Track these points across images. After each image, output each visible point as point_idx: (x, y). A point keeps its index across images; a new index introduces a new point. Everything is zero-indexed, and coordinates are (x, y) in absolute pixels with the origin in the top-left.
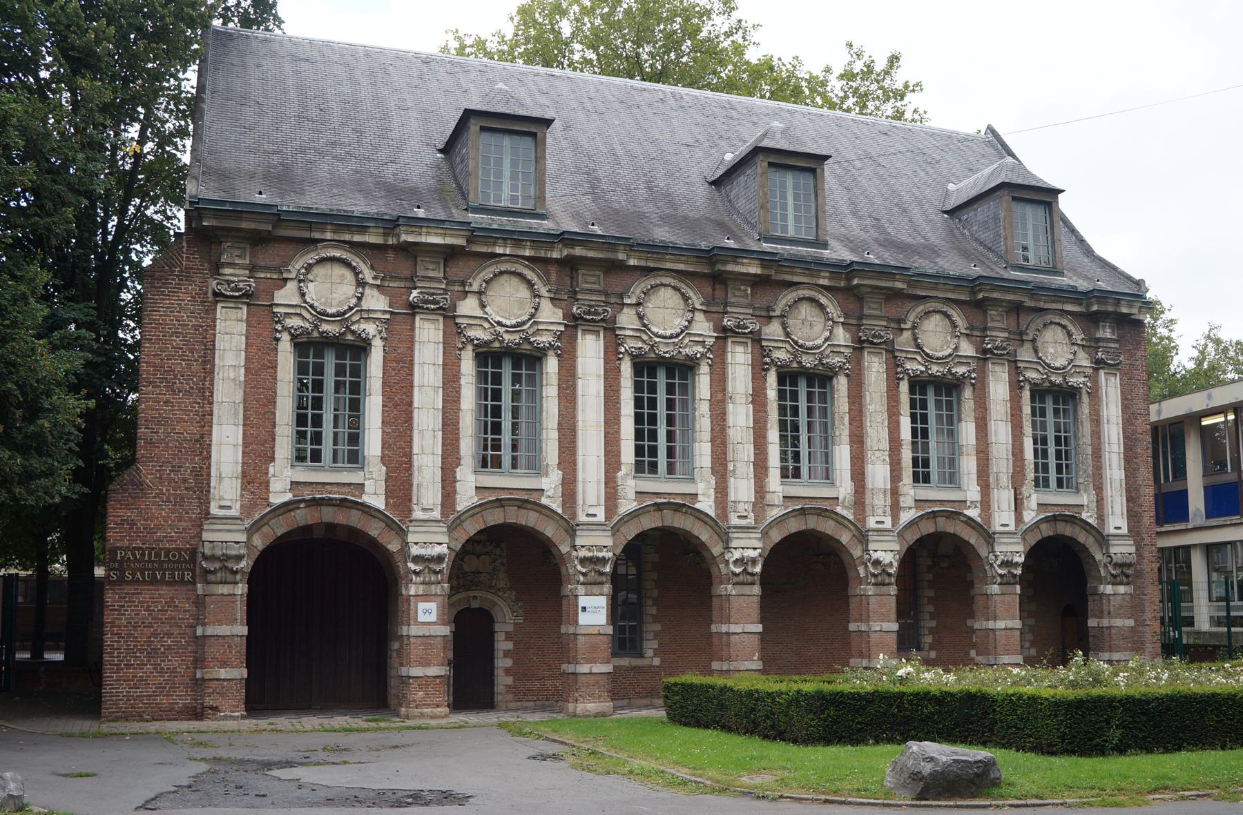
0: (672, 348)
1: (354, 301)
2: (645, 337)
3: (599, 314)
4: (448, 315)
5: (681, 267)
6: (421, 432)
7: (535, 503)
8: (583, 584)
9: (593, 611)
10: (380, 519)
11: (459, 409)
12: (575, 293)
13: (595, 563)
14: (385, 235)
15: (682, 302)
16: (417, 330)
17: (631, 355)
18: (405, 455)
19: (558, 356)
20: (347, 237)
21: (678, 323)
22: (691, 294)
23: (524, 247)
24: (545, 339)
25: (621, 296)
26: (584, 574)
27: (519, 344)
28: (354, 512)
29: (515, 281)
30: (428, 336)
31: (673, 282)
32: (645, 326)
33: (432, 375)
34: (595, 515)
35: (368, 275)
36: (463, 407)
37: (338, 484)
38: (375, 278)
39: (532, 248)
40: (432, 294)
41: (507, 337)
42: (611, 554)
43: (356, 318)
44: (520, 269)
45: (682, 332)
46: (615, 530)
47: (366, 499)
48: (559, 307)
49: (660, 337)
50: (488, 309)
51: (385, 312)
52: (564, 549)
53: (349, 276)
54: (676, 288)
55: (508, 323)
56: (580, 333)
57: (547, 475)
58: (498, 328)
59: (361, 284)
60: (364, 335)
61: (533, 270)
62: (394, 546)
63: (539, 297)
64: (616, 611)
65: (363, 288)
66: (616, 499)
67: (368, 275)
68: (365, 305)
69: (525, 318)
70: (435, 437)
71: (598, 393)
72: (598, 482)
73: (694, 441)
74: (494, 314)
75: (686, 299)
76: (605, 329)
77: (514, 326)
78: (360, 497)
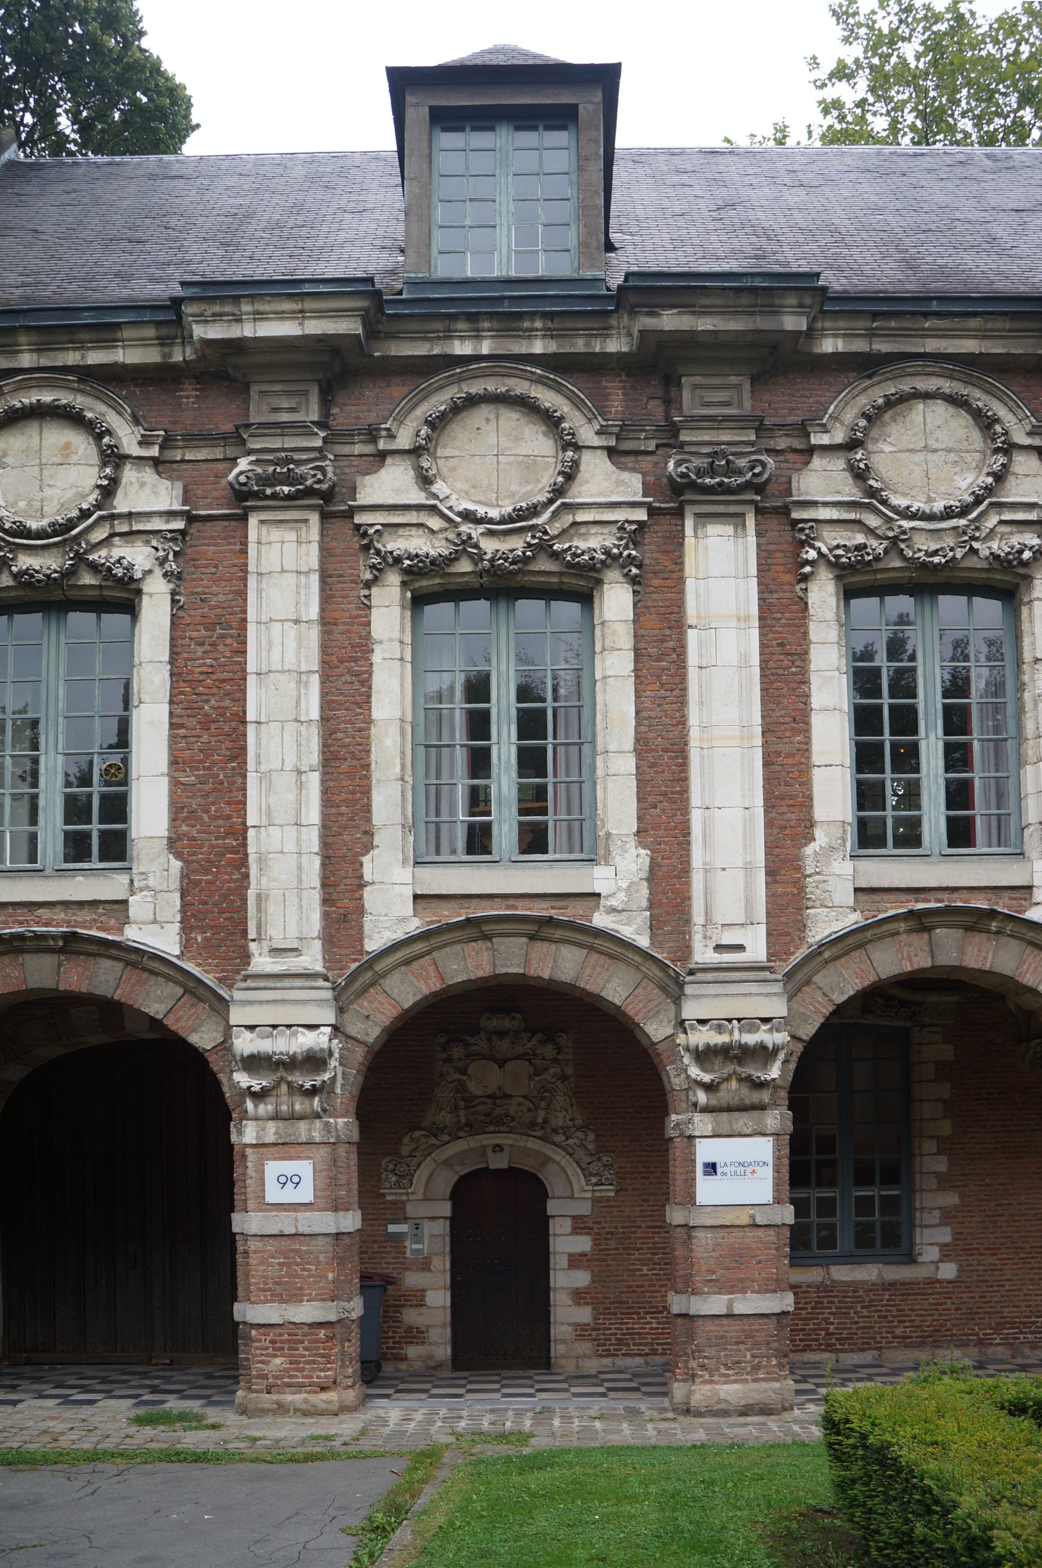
0: (950, 541)
1: (94, 497)
2: (873, 521)
3: (740, 472)
4: (332, 505)
5: (970, 346)
6: (265, 777)
7: (571, 926)
9: (736, 1172)
10: (169, 978)
11: (369, 721)
12: (674, 430)
14: (163, 341)
15: (976, 436)
16: (252, 549)
17: (835, 565)
18: (230, 833)
19: (634, 581)
20: (72, 358)
21: (965, 483)
22: (1002, 412)
23: (529, 334)
24: (594, 543)
25: (803, 430)
26: (710, 1088)
27: (525, 560)
28: (106, 964)
29: (510, 418)
30: (283, 564)
31: (947, 386)
32: (872, 493)
33: (291, 646)
34: (740, 948)
35: (128, 437)
36: (376, 714)
37: (66, 904)
38: (144, 442)
39: (550, 334)
40: (288, 461)
41: (489, 546)
42: (781, 1037)
43: (99, 535)
44: (520, 387)
45: (978, 502)
46: (796, 982)
47: (132, 934)
48: (633, 470)
49: (914, 516)
50: (440, 487)
51: (170, 514)
52: (657, 1030)
53: (81, 444)
54: (956, 401)
55: (494, 513)
56: (689, 524)
57: (607, 860)
58: (465, 528)
59: (113, 458)
60: (119, 572)
61: (557, 388)
62: (203, 1038)
63: (578, 448)
64: (804, 1166)
65: (118, 467)
66: (800, 909)
67: (128, 437)
68: (121, 504)
69: (543, 498)
70: (301, 786)
71: (744, 658)
72: (748, 868)
73: (1021, 762)
74: (454, 493)
75: (986, 423)
76: (760, 512)
77: (511, 520)
78: (120, 930)
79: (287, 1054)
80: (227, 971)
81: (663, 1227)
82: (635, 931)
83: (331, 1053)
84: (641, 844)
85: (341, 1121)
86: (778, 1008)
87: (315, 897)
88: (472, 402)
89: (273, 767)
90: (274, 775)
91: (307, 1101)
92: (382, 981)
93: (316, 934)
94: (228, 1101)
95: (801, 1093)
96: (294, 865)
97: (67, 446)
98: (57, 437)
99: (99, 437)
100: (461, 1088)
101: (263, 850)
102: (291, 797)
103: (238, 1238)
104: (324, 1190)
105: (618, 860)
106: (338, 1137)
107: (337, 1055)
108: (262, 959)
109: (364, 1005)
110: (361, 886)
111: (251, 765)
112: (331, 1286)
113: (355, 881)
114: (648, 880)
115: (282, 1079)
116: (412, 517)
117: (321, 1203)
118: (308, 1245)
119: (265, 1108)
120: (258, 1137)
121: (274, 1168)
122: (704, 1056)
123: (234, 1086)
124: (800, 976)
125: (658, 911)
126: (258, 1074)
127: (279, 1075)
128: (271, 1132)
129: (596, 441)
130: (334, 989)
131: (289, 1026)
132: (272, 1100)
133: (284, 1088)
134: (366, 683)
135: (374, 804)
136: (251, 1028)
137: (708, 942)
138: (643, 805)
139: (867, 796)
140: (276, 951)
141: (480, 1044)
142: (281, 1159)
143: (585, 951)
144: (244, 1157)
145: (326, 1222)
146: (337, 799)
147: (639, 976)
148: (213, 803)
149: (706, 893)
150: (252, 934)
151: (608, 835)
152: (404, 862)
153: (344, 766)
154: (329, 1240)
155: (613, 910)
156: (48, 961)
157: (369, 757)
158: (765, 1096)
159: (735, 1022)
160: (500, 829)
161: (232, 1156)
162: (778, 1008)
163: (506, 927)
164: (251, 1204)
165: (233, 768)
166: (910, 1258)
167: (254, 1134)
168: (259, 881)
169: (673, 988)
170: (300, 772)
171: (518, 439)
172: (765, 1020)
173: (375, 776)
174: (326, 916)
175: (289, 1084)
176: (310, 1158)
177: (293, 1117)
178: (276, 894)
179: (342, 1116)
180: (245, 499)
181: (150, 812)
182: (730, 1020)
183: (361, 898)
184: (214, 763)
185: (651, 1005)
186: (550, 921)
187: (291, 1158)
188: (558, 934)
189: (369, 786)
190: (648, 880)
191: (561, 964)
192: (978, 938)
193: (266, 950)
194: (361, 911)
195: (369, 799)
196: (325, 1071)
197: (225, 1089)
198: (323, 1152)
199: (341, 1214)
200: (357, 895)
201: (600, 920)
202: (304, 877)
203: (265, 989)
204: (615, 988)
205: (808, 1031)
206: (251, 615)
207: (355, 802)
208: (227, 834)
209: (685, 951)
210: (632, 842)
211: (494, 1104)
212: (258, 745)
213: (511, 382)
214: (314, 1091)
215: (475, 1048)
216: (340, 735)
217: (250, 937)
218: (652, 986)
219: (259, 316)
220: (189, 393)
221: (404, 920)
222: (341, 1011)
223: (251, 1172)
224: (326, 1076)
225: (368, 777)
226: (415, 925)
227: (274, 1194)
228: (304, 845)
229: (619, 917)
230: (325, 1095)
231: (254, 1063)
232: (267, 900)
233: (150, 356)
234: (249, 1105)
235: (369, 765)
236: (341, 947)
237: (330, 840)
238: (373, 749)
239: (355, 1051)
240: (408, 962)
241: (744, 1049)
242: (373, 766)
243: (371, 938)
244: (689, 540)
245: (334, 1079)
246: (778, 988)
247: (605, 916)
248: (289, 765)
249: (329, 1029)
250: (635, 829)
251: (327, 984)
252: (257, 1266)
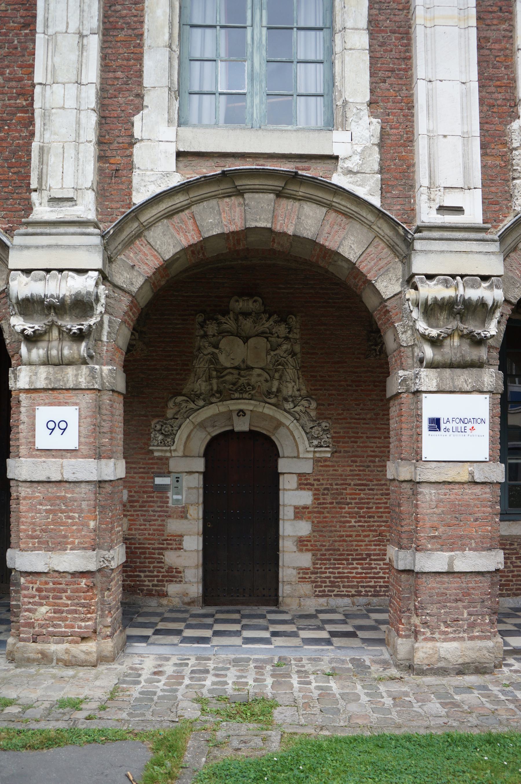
6: (52, 39)
8: (432, 365)
13: (462, 316)
42: (499, 295)
52: (388, 286)
70: (82, 48)
79: (58, 298)
80: (13, 223)
81: (386, 485)
82: (368, 190)
83: (97, 300)
84: (372, 114)
85: (106, 369)
86: (495, 266)
87: (90, 151)
89: (58, 29)
90: (60, 37)
91: (75, 347)
92: (146, 233)
93: (89, 185)
94: (8, 347)
96: (73, 119)
100: (214, 360)
101: (47, 106)
102: (74, 57)
103: (12, 483)
104: (87, 437)
105: (353, 127)
106: (103, 384)
107: (103, 301)
108: (42, 209)
109: (130, 256)
110: (131, 145)
111: (40, 27)
112: (92, 535)
113: (127, 140)
114: (378, 145)
115: (52, 324)
117: (85, 450)
118: (73, 492)
119: (38, 353)
120: (31, 382)
121: (45, 414)
122: (431, 309)
123: (12, 332)
125: (387, 176)
126: (32, 319)
127: (50, 319)
128: (42, 377)
130: (103, 237)
131: (61, 271)
132: (43, 344)
133: (55, 333)
135: (145, 69)
136: (27, 272)
137: (432, 204)
138: (374, 79)
140: (55, 201)
141: (229, 324)
142: (51, 404)
143: (324, 210)
145: (88, 469)
146: (114, 64)
147: (371, 235)
148: (8, 67)
149: (430, 158)
150: (34, 185)
151: (345, 103)
152: (170, 121)
153: (121, 36)
154: (91, 487)
155: (350, 172)
157: (142, 27)
158: (483, 353)
159: (458, 278)
160: (252, 102)
161: (9, 402)
162: (495, 266)
163: (256, 182)
164: (23, 450)
165: (26, 35)
167: (27, 379)
168: (42, 135)
169: (402, 247)
170: (82, 36)
172: (485, 278)
173: (147, 41)
174: (100, 171)
175: (59, 327)
176: (76, 404)
177: (62, 363)
178: (56, 148)
179: (107, 364)
182: (454, 276)
183: (131, 155)
184: (10, 30)
185: (382, 263)
187: (59, 404)
188: (302, 191)
189: (142, 53)
190: (378, 145)
191: (304, 220)
193: (46, 199)
194: (130, 167)
195: (141, 65)
196: (91, 317)
197: (6, 336)
198: (88, 398)
199: (103, 461)
200: (128, 152)
201: (338, 179)
202: (82, 132)
203: (41, 234)
204: (351, 244)
207: (130, 68)
208: (19, 94)
209: (411, 212)
210: (365, 111)
211: (239, 374)
212: (47, 9)
214: (80, 336)
215: (225, 326)
216: (119, 7)
217: (33, 187)
218: (382, 245)
221: (167, 175)
222: (109, 260)
223: (23, 417)
224: (92, 321)
225: (141, 46)
226: (176, 180)
227: (44, 440)
228: (83, 102)
229: (355, 178)
230: (92, 342)
231: (29, 306)
232: (48, 152)
234: (24, 349)
235: (142, 35)
236: (112, 201)
237: (106, 102)
238: (146, 21)
239: (121, 301)
240: (170, 215)
241: (467, 304)
242: (146, 34)
243: (138, 191)
245: (101, 324)
246: (495, 247)
247: (342, 177)
248: (72, 28)
249: (96, 273)
250: (368, 98)
251: (97, 231)
252: (28, 512)
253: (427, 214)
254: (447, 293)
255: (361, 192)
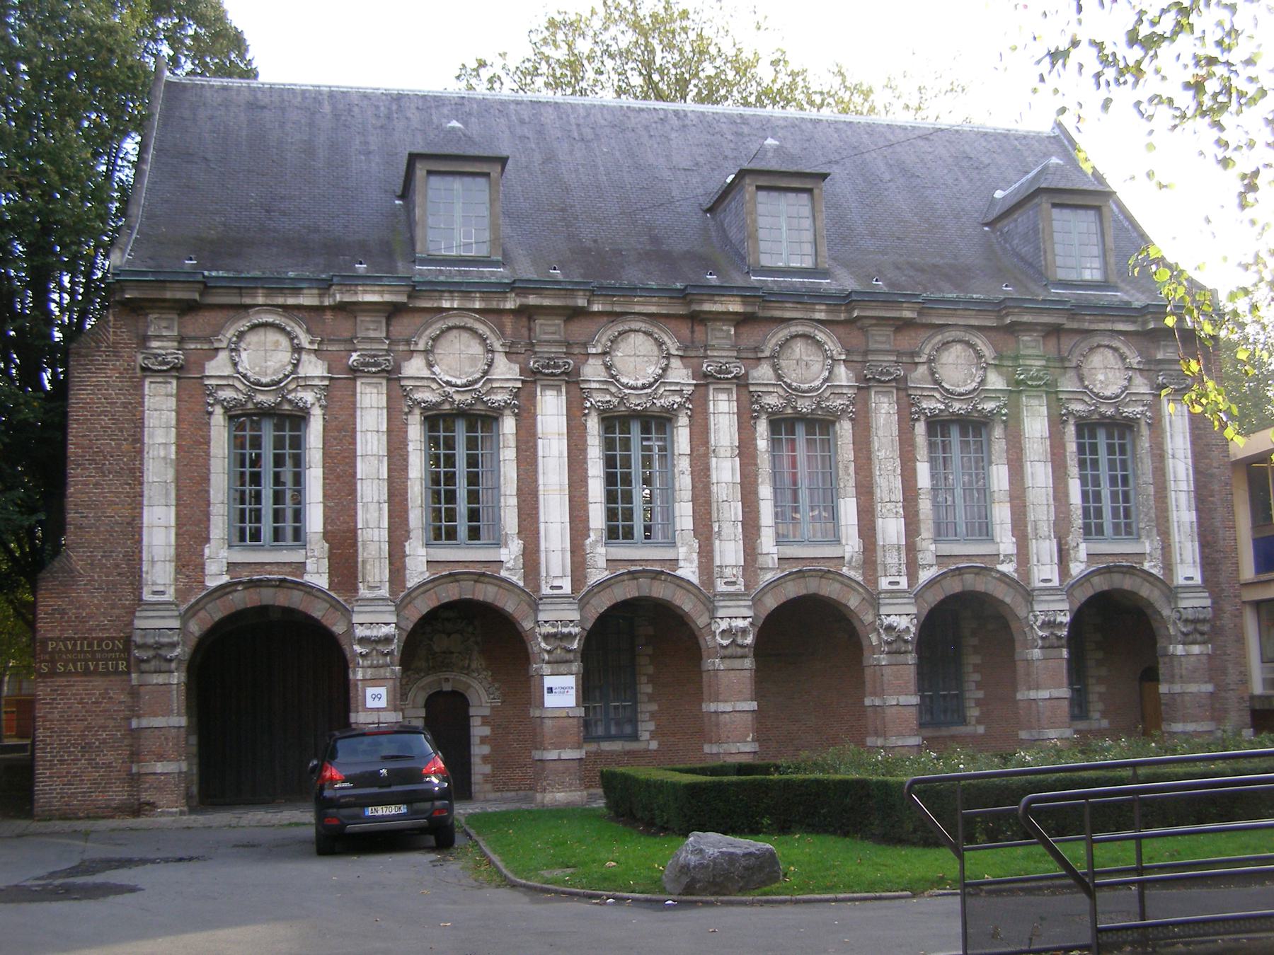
1: (289, 368)
4: (391, 375)
9: (561, 692)
10: (325, 600)
11: (407, 478)
13: (561, 639)
14: (321, 296)
16: (358, 396)
19: (516, 415)
24: (500, 397)
26: (549, 652)
27: (472, 404)
28: (296, 593)
29: (465, 336)
33: (376, 443)
35: (304, 339)
40: (374, 356)
41: (457, 397)
43: (292, 386)
46: (583, 604)
47: (307, 578)
51: (323, 378)
52: (527, 625)
53: (284, 342)
55: (459, 382)
57: (506, 545)
58: (448, 389)
59: (298, 349)
60: (301, 404)
61: (484, 323)
62: (339, 629)
63: (493, 352)
65: (299, 354)
67: (304, 339)
68: (302, 372)
69: (477, 376)
71: (561, 453)
72: (563, 550)
77: (466, 386)
78: (302, 577)
82: (517, 579)
84: (520, 538)
88: (450, 329)
95: (586, 654)
97: (277, 341)
98: (272, 337)
99: (292, 339)
116: (425, 383)
122: (547, 637)
124: (585, 600)
129: (501, 349)
134: (406, 460)
139: (611, 515)
144: (356, 685)
155: (508, 569)
156: (272, 590)
166: (635, 737)
171: (468, 346)
180: (355, 372)
181: (315, 520)
186: (483, 574)
188: (487, 580)
192: (657, 583)
201: (503, 574)
204: (510, 605)
205: (589, 625)
206: (358, 428)
213: (466, 319)
219: (365, 292)
220: (329, 316)
233: (313, 301)
244: (539, 397)
253: (546, 590)
254: (553, 630)
255: (514, 579)
